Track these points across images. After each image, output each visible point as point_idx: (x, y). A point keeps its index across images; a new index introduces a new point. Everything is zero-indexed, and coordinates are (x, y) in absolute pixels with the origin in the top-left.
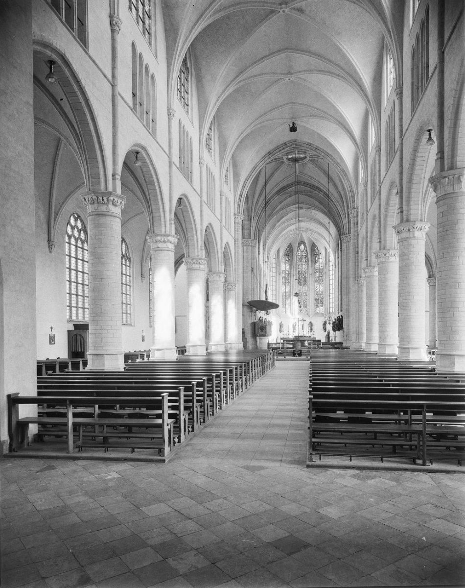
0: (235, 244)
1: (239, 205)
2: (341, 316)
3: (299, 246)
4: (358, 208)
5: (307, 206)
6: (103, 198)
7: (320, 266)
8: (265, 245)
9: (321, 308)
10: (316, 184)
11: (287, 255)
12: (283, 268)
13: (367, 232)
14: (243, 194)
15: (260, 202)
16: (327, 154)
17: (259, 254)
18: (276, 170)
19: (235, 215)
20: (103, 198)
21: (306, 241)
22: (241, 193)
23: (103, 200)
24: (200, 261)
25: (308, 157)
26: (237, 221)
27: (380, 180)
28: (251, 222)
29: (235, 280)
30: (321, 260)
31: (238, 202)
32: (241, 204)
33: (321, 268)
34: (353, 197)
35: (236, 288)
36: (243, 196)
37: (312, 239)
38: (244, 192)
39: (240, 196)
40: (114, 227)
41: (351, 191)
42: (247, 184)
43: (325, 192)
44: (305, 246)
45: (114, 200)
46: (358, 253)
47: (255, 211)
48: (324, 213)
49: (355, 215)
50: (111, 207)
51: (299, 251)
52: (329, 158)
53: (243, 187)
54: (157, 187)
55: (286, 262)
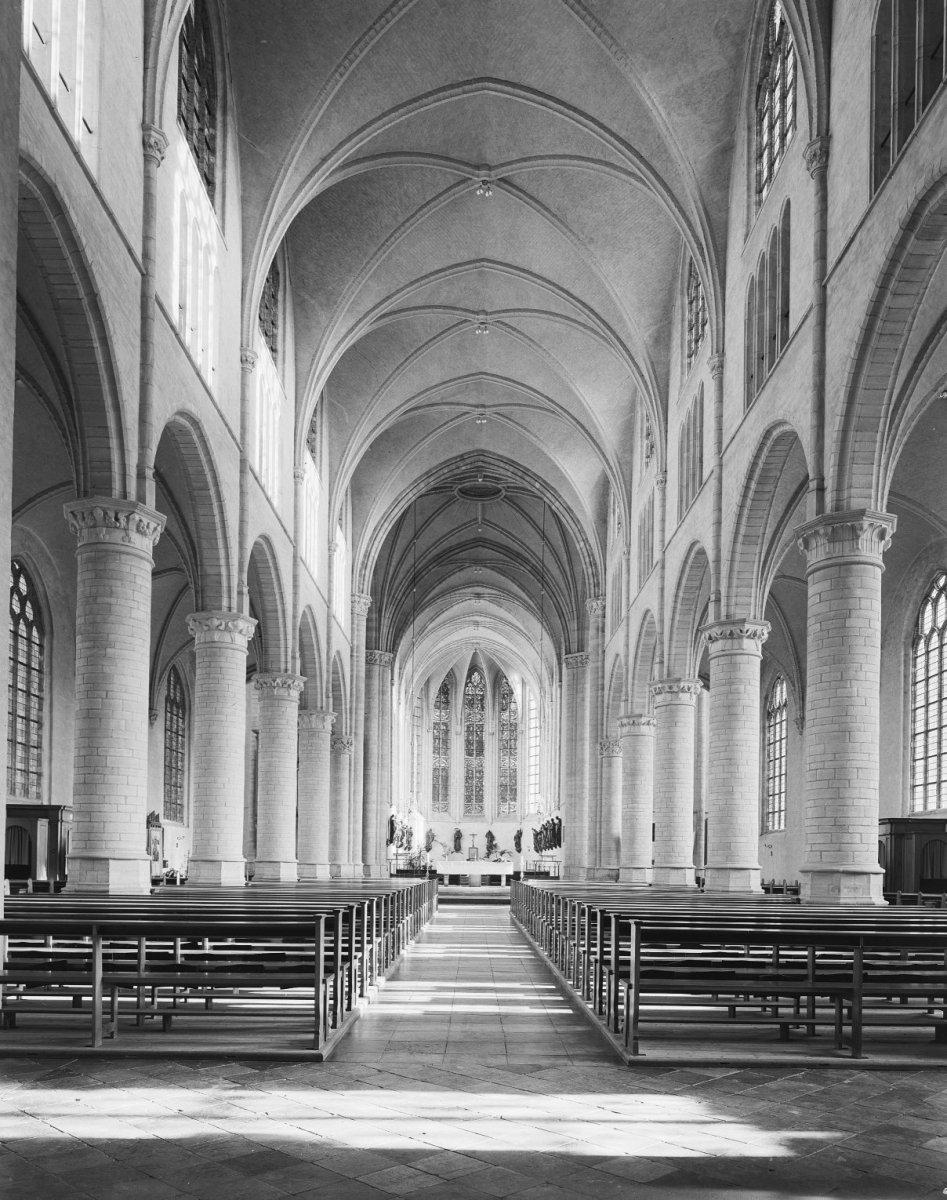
0: (352, 656)
4: (604, 600)
5: (494, 592)
6: (116, 514)
10: (516, 547)
13: (627, 646)
14: (372, 554)
15: (401, 576)
16: (546, 485)
17: (392, 685)
20: (116, 514)
21: (484, 666)
22: (366, 551)
23: (117, 519)
26: (357, 610)
27: (663, 541)
31: (360, 571)
32: (367, 574)
34: (595, 575)
36: (371, 558)
37: (498, 663)
39: (365, 556)
40: (139, 581)
41: (593, 564)
42: (381, 534)
45: (141, 521)
46: (603, 689)
48: (528, 608)
49: (600, 612)
50: (135, 536)
52: (549, 495)
53: (373, 539)
54: (216, 511)
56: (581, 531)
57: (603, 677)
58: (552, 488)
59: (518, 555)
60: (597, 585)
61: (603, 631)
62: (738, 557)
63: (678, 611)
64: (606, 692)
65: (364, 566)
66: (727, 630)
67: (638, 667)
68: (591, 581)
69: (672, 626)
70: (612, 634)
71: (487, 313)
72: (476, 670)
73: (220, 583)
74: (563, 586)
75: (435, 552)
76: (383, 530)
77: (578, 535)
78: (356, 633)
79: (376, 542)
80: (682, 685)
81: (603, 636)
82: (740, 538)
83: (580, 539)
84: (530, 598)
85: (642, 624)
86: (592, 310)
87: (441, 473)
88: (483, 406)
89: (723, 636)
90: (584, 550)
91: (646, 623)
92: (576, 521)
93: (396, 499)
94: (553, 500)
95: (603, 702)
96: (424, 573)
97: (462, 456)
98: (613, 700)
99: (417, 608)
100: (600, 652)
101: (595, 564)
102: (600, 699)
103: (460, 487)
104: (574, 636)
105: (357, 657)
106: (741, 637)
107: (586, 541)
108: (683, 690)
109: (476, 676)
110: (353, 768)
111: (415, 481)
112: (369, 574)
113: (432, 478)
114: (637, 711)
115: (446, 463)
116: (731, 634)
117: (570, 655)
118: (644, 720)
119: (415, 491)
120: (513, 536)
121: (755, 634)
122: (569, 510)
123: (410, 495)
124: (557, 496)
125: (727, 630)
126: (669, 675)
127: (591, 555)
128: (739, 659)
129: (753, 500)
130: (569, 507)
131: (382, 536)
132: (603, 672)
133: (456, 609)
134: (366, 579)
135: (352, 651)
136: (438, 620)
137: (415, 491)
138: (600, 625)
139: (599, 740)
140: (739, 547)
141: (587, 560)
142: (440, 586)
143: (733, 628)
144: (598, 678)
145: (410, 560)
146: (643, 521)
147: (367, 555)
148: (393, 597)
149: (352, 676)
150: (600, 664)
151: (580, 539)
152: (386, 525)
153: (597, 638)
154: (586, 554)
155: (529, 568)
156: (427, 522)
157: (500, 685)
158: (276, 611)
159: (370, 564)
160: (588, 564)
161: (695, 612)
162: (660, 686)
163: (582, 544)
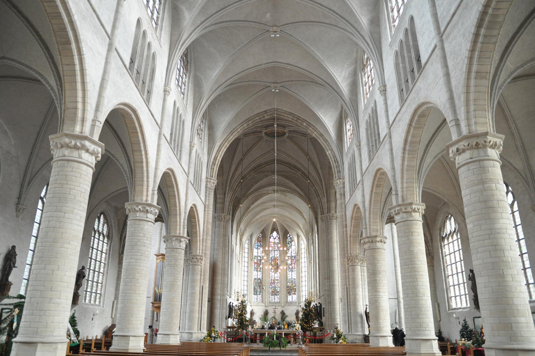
0: (205, 210)
1: (212, 169)
2: (319, 303)
3: (272, 233)
4: (344, 179)
7: (293, 253)
8: (238, 226)
9: (294, 296)
10: (294, 162)
11: (260, 241)
12: (255, 254)
13: (363, 196)
14: (218, 158)
15: (236, 177)
16: (309, 124)
17: (232, 234)
18: (254, 145)
19: (207, 178)
21: (279, 228)
22: (215, 157)
24: (148, 208)
25: (287, 134)
26: (209, 186)
28: (225, 197)
29: (202, 252)
30: (293, 247)
31: (212, 166)
32: (215, 168)
33: (293, 255)
34: (338, 167)
35: (203, 262)
36: (217, 160)
37: (285, 226)
38: (219, 156)
39: (214, 159)
41: (336, 161)
42: (223, 148)
43: (303, 171)
44: (278, 233)
46: (346, 227)
47: (230, 186)
48: (300, 196)
49: (341, 186)
51: (272, 237)
52: (310, 129)
53: (219, 151)
54: (77, 61)
55: (259, 247)
56: (329, 145)
57: (346, 220)
58: (312, 125)
59: (295, 167)
60: (339, 172)
61: (344, 195)
62: (472, 89)
63: (406, 159)
64: (348, 228)
65: (214, 164)
66: (474, 142)
67: (372, 207)
68: (336, 170)
69: (402, 170)
70: (351, 195)
71: (277, 27)
72: (275, 230)
73: (75, 114)
74: (318, 181)
75: (253, 166)
76: (224, 146)
77: (327, 147)
78: (208, 198)
79: (220, 153)
80: (414, 206)
81: (345, 198)
82: (473, 75)
83: (328, 149)
84: (301, 191)
85: (374, 180)
86: (334, 11)
87: (255, 119)
88: (275, 83)
89: (470, 147)
90: (331, 154)
91: (377, 179)
92: (326, 141)
93: (232, 132)
94: (313, 131)
95: (347, 234)
96: (247, 176)
97: (266, 111)
98: (353, 232)
99: (245, 196)
100: (343, 207)
101: (337, 162)
102: (345, 233)
103: (265, 131)
104: (325, 206)
105: (208, 211)
106: (485, 147)
107: (332, 150)
108: (414, 211)
109: (275, 234)
110: (203, 274)
111: (242, 123)
112: (216, 168)
113: (250, 122)
114: (373, 234)
115: (258, 115)
116: (477, 144)
117: (324, 215)
118: (378, 239)
119: (242, 128)
120: (292, 157)
121: (496, 145)
122: (322, 135)
123: (239, 130)
124: (315, 129)
125: (474, 142)
126: (403, 200)
127: (335, 157)
128: (486, 163)
129: (483, 43)
130: (322, 134)
131: (224, 150)
132: (346, 217)
133: (265, 198)
134: (215, 170)
135: (205, 208)
136: (256, 204)
137: (242, 128)
138: (342, 192)
139: (346, 255)
140: (472, 82)
141: (333, 159)
142: (256, 185)
143: (478, 140)
144: (343, 221)
145: (240, 170)
146: (368, 124)
147: (215, 158)
148: (232, 187)
149: (204, 221)
150: (343, 213)
151: (328, 149)
152: (226, 144)
153: (341, 199)
154: (332, 157)
155: (300, 173)
156: (249, 151)
157: (287, 238)
158: (142, 162)
159: (217, 163)
160: (334, 162)
161: (417, 160)
162: (399, 208)
163: (330, 152)
